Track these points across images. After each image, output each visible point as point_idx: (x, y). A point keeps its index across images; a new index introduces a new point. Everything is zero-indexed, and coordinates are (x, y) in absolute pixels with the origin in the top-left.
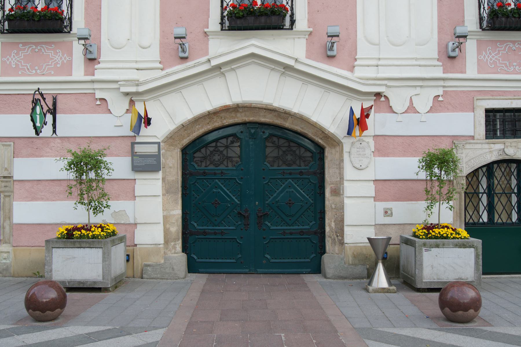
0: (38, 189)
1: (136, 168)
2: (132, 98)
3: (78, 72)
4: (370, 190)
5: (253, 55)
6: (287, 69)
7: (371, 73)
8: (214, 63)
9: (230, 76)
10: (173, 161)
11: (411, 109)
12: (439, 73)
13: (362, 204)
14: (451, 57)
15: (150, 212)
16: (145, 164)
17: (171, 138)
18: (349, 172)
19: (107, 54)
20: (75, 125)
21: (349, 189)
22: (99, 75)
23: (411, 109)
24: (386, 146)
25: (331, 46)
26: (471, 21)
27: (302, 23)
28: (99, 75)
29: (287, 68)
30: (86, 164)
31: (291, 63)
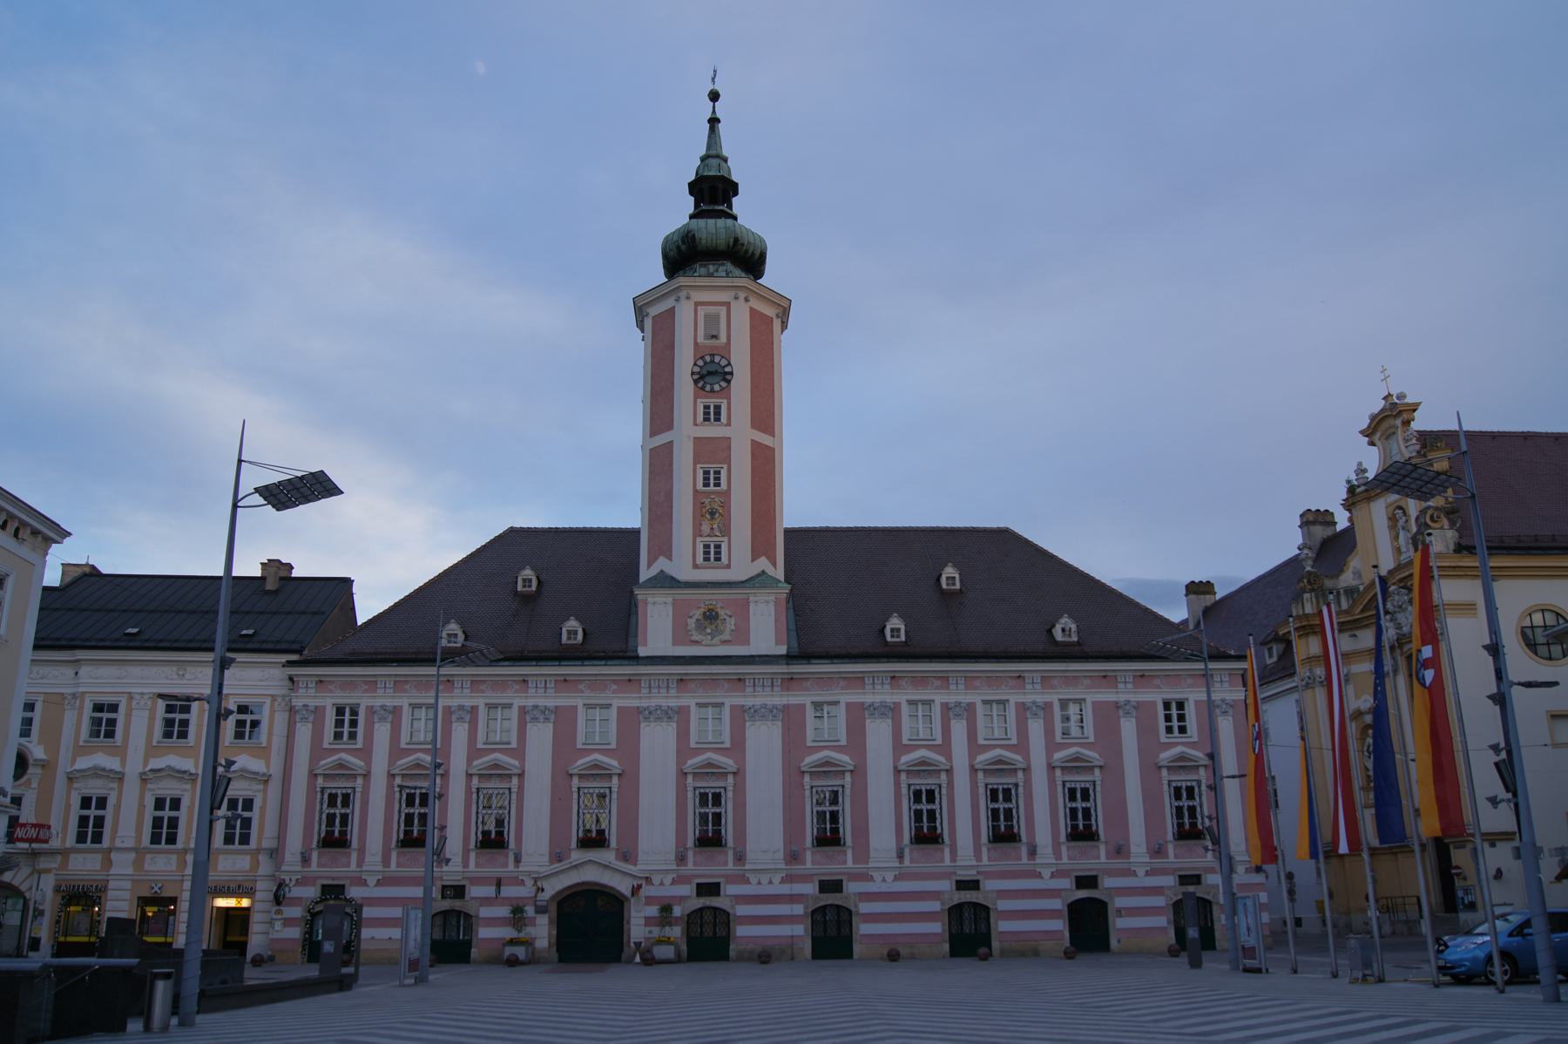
0: (491, 922)
1: (537, 912)
2: (536, 880)
3: (511, 867)
4: (643, 921)
6: (606, 867)
10: (553, 908)
11: (662, 884)
13: (638, 927)
14: (681, 859)
15: (542, 932)
16: (540, 910)
17: (553, 897)
18: (633, 913)
20: (508, 891)
21: (633, 921)
23: (662, 884)
24: (650, 901)
25: (628, 856)
26: (690, 842)
27: (613, 844)
29: (606, 867)
30: (518, 911)
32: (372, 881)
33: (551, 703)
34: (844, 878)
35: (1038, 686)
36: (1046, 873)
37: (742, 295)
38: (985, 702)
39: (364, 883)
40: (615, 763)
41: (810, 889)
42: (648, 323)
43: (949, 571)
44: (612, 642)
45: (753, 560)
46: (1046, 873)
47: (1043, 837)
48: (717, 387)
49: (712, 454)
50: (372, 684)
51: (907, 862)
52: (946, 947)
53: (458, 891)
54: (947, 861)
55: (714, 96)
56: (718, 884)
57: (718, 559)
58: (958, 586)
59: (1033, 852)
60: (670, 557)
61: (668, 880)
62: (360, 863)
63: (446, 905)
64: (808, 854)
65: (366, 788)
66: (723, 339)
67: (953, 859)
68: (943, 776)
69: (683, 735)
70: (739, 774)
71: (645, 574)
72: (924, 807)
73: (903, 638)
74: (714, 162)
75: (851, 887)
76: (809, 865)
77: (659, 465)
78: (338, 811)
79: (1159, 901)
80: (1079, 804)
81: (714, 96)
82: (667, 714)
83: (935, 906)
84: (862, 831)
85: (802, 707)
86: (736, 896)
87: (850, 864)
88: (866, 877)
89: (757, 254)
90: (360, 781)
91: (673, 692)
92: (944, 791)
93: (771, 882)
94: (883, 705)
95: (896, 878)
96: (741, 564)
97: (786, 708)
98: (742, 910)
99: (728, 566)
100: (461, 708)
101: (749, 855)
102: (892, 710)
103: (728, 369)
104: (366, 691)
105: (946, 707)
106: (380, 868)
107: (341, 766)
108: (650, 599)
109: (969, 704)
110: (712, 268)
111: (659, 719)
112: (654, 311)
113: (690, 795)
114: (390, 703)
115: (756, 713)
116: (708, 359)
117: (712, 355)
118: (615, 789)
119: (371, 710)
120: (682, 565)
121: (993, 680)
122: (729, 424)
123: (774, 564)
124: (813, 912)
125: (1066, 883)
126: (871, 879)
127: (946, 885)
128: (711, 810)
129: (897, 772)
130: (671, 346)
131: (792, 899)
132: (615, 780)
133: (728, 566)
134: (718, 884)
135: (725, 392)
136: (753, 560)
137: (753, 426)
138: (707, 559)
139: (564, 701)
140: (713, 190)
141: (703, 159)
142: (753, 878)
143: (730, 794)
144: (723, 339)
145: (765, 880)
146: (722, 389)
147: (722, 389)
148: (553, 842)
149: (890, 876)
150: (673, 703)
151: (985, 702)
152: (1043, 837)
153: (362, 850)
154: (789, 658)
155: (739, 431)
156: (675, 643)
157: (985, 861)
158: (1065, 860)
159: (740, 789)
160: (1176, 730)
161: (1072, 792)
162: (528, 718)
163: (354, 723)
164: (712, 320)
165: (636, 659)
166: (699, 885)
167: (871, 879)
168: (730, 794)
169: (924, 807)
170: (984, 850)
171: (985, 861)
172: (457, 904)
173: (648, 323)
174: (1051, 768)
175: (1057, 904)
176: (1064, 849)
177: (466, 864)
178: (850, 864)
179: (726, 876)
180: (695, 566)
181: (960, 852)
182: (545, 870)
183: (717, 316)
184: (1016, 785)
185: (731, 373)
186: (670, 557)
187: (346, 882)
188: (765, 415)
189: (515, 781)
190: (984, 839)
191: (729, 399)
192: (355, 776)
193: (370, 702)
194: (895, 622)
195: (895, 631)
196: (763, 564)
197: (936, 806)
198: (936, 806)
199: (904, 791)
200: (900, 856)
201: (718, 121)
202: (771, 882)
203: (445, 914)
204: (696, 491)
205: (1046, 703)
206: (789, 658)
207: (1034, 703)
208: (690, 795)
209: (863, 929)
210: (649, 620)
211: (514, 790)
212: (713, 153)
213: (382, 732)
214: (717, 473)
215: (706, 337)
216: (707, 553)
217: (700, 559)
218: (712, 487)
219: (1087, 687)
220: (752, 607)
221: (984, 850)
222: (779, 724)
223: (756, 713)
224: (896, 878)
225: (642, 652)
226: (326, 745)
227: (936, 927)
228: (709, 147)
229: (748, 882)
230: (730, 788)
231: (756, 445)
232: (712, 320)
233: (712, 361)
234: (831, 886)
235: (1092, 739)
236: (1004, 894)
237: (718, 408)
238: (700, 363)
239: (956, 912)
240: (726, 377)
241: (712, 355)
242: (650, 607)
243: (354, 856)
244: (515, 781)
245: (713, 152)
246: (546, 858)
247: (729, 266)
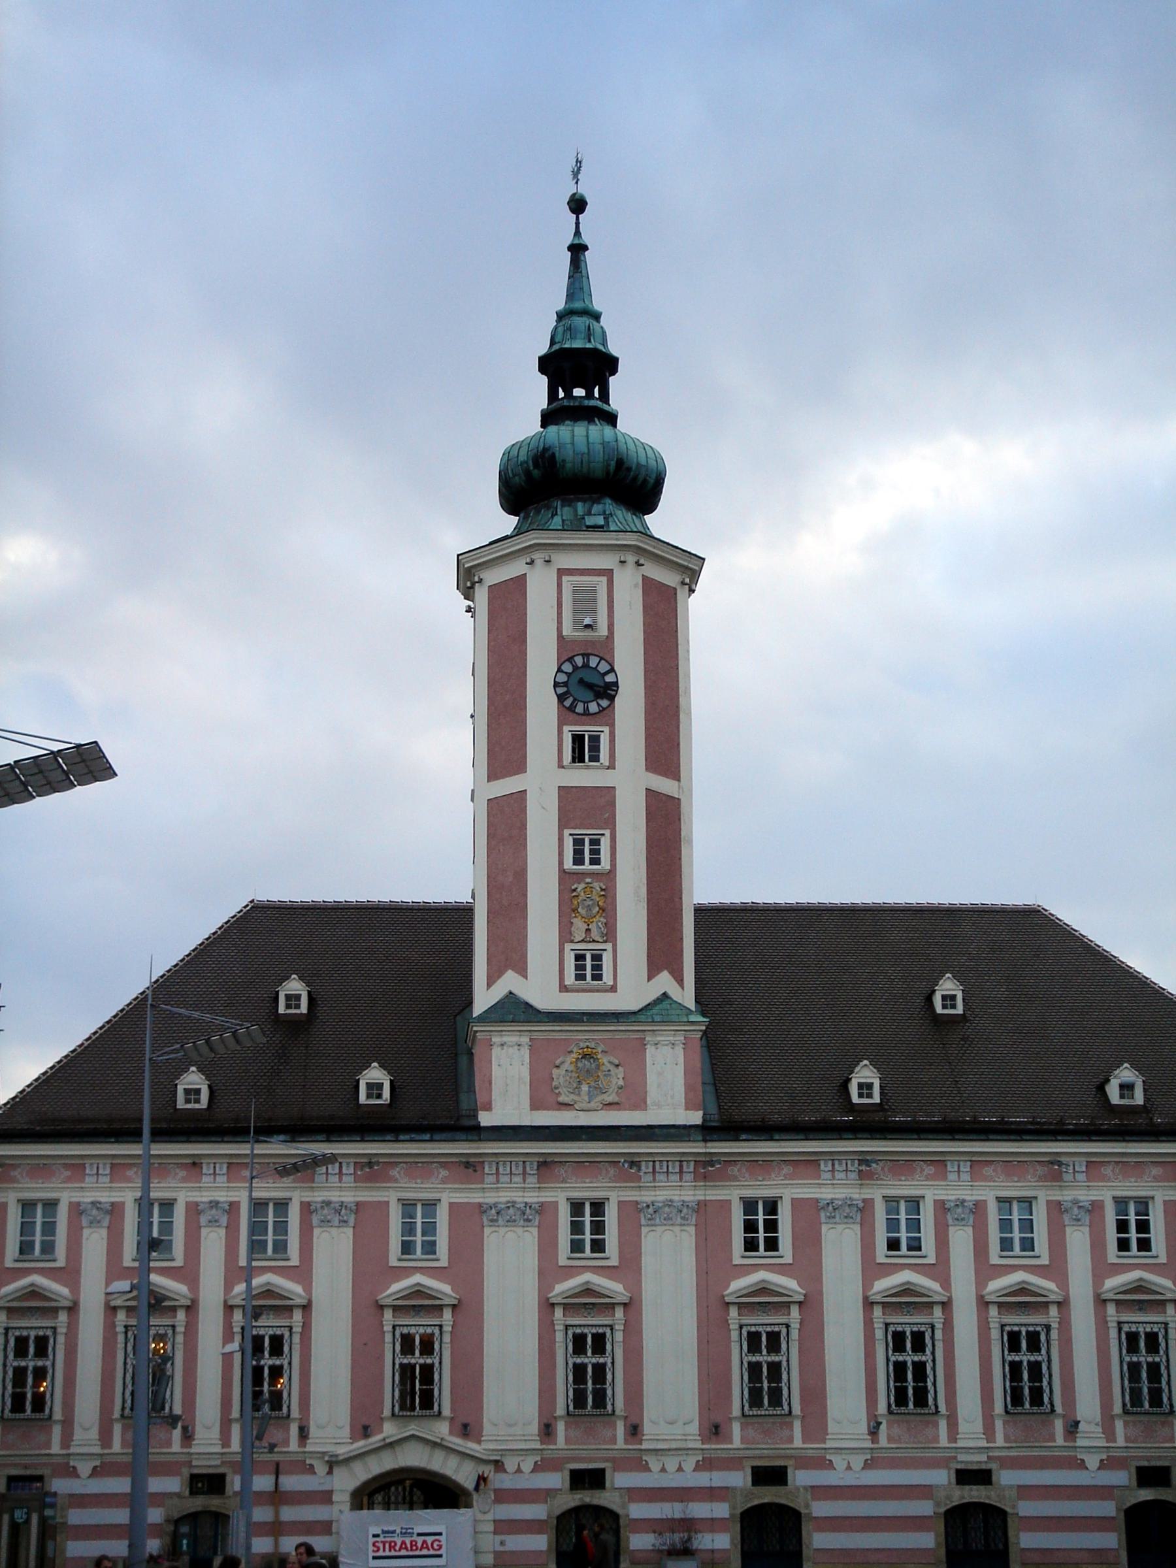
3: (294, 1445)
5: (413, 1436)
7: (492, 1446)
8: (388, 1441)
9: (398, 1449)
11: (519, 1470)
12: (538, 1446)
14: (547, 1431)
19: (313, 1431)
22: (309, 1448)
23: (519, 1470)
27: (446, 1412)
28: (309, 1448)
29: (435, 1445)
31: (438, 1441)
32: (84, 1468)
33: (349, 1197)
34: (790, 1463)
35: (1081, 1177)
36: (1092, 1462)
37: (631, 558)
38: (1000, 1200)
39: (73, 1473)
40: (446, 1288)
41: (740, 1479)
42: (482, 594)
43: (948, 985)
44: (437, 1106)
45: (649, 979)
46: (1092, 1462)
47: (1088, 1406)
48: (593, 707)
49: (586, 811)
50: (77, 1168)
51: (883, 1441)
53: (212, 1483)
54: (944, 1441)
55: (578, 205)
56: (603, 1471)
57: (597, 977)
58: (959, 1010)
59: (1072, 1428)
60: (523, 971)
61: (527, 1466)
62: (66, 1441)
63: (198, 1503)
64: (736, 1428)
65: (73, 1327)
66: (603, 631)
67: (953, 1437)
68: (938, 1312)
69: (547, 1247)
70: (631, 1305)
71: (484, 998)
72: (909, 1358)
73: (877, 1099)
74: (580, 322)
75: (800, 1478)
76: (737, 1442)
77: (504, 825)
78: (30, 1363)
80: (1143, 1358)
81: (578, 205)
82: (524, 1214)
83: (925, 1508)
84: (815, 1396)
85: (725, 1205)
86: (629, 1490)
87: (798, 1442)
88: (822, 1463)
89: (652, 481)
90: (63, 1317)
91: (532, 1180)
92: (939, 1334)
93: (680, 1469)
94: (849, 1203)
95: (867, 1465)
96: (631, 983)
97: (701, 1206)
98: (638, 1511)
99: (613, 989)
100: (214, 1204)
101: (647, 1428)
102: (861, 1210)
103: (609, 678)
104: (68, 1180)
105: (941, 1207)
106: (97, 1450)
107: (34, 1293)
108: (496, 1039)
109: (977, 1204)
110: (580, 507)
111: (511, 1222)
112: (493, 577)
113: (559, 1336)
114: (105, 1197)
115: (654, 1211)
116: (579, 661)
117: (586, 656)
118: (447, 1329)
119: (77, 1210)
120: (540, 986)
121: (1012, 1166)
122: (612, 766)
123: (680, 981)
125: (1121, 1478)
127: (941, 1477)
128: (589, 1359)
129: (869, 1304)
130: (521, 638)
131: (712, 1494)
132: (447, 1315)
133: (613, 989)
134: (603, 1471)
135: (606, 715)
136: (649, 979)
137: (647, 769)
138: (580, 977)
139: (367, 1196)
140: (578, 370)
141: (561, 316)
142: (655, 1465)
143: (619, 1336)
144: (603, 631)
145: (672, 1465)
146: (602, 710)
147: (602, 710)
148: (356, 1408)
149: (858, 1461)
150: (533, 1198)
151: (1000, 1200)
152: (1088, 1406)
153: (68, 1423)
154: (707, 1131)
155: (626, 775)
156: (536, 1105)
157: (1000, 1441)
159: (633, 1329)
161: (1132, 1338)
162: (315, 1220)
164: (585, 600)
165: (476, 1132)
167: (830, 1465)
168: (619, 1336)
169: (909, 1358)
170: (999, 1424)
171: (1000, 1441)
172: (214, 1503)
173: (482, 594)
174: (1101, 1302)
175: (1108, 1509)
176: (1119, 1425)
178: (798, 1442)
179: (613, 1460)
180: (564, 988)
181: (963, 1427)
182: (342, 1451)
183: (593, 593)
184: (1048, 1328)
185: (616, 684)
186: (523, 971)
187: (46, 1472)
188: (665, 748)
189: (298, 1316)
190: (999, 1408)
191: (612, 726)
192: (55, 1311)
193: (76, 1197)
194: (865, 1073)
195: (865, 1088)
196: (664, 982)
197: (926, 1357)
198: (926, 1357)
199: (879, 1334)
200: (874, 1432)
201: (585, 248)
202: (680, 1469)
203: (193, 1518)
204: (563, 872)
205: (1093, 1203)
206: (707, 1131)
207: (1075, 1202)
208: (559, 1336)
210: (496, 1072)
211: (297, 1329)
212: (577, 311)
213: (95, 1243)
214: (595, 842)
215: (575, 629)
216: (580, 968)
217: (570, 979)
218: (587, 866)
219: (1156, 1179)
220: (650, 1050)
221: (999, 1424)
222: (692, 1230)
223: (654, 1211)
224: (867, 1465)
225: (486, 1119)
226: (9, 1263)
228: (570, 296)
229: (646, 1468)
230: (619, 1327)
231: (652, 795)
232: (585, 600)
233: (586, 665)
234: (770, 1475)
235: (1163, 1259)
236: (1026, 1492)
237: (595, 739)
238: (568, 667)
239: (958, 1518)
240: (607, 691)
241: (586, 656)
242: (496, 1051)
243: (57, 1431)
244: (298, 1316)
245: (578, 305)
246: (346, 1432)
247: (608, 505)
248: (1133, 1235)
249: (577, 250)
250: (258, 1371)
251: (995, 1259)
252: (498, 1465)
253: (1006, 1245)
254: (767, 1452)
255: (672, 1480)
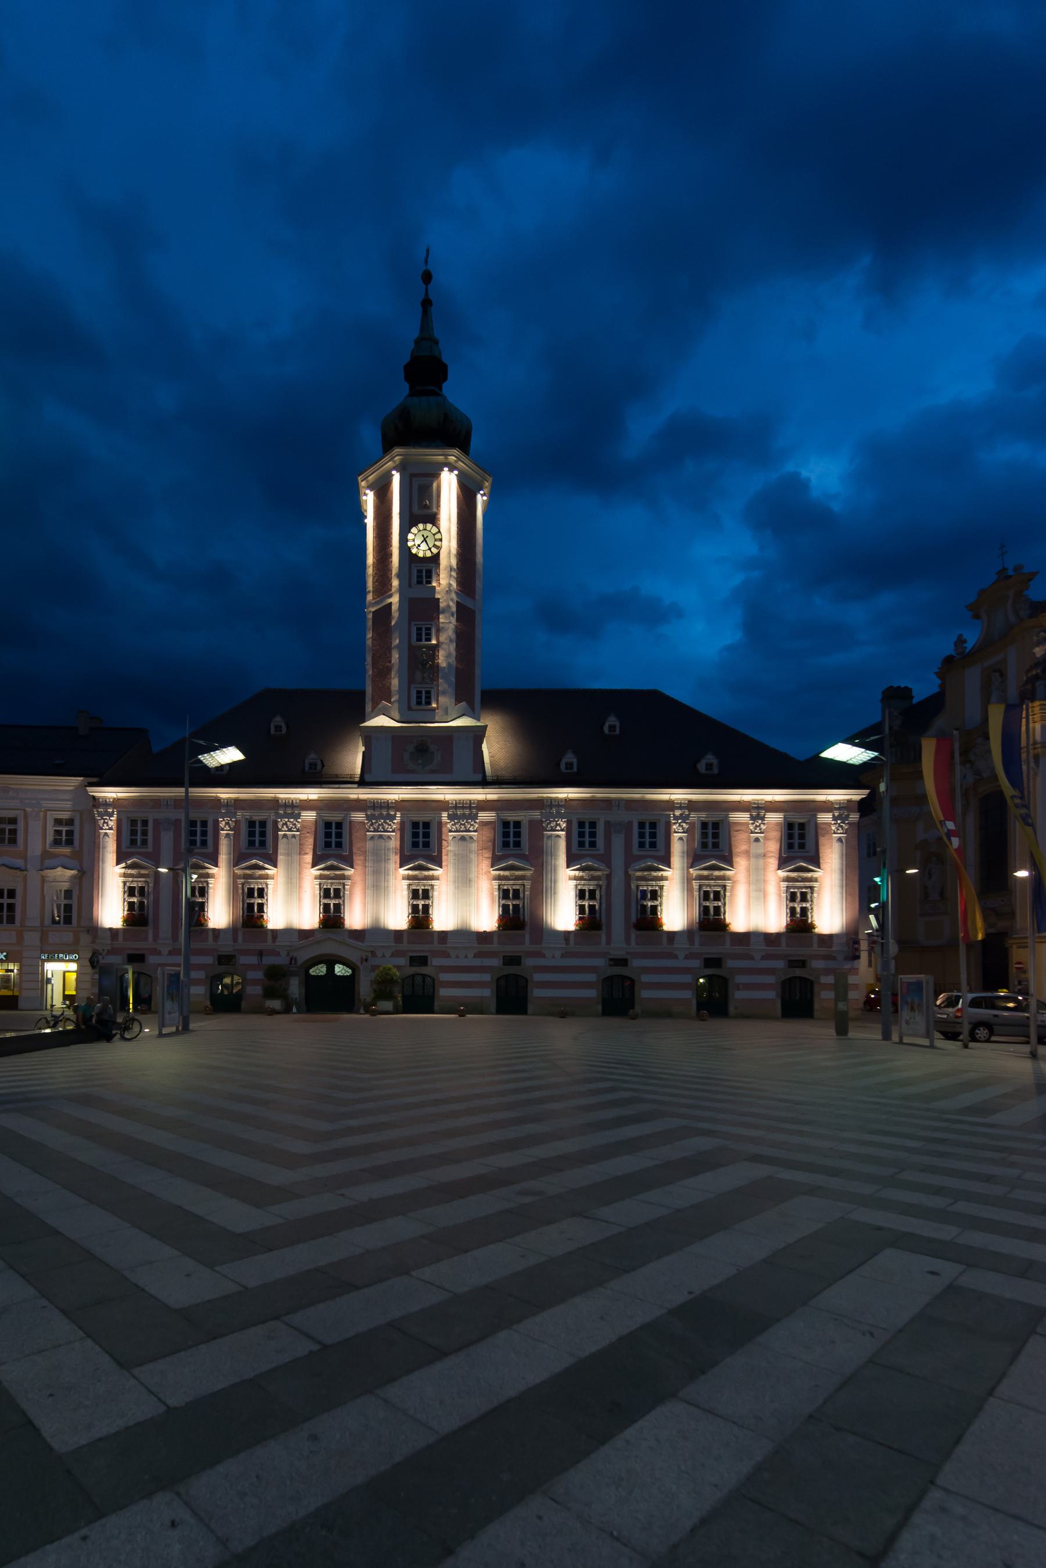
11: (384, 956)
20: (269, 960)
23: (384, 956)
41: (496, 962)
52: (600, 1007)
62: (156, 937)
75: (529, 962)
79: (771, 979)
83: (592, 977)
88: (539, 954)
95: (563, 956)
98: (444, 977)
119: (156, 822)
124: (498, 980)
126: (543, 956)
138: (419, 703)
153: (156, 928)
156: (394, 771)
158: (697, 945)
160: (796, 846)
163: (145, 833)
166: (411, 957)
167: (543, 956)
177: (235, 940)
202: (466, 957)
204: (410, 645)
209: (537, 993)
216: (419, 697)
224: (563, 956)
227: (592, 993)
229: (448, 956)
234: (513, 960)
239: (609, 982)
248: (647, 840)
249: (426, 303)
250: (251, 906)
251: (636, 851)
252: (373, 954)
253: (641, 845)
254: (511, 949)
255: (463, 962)
